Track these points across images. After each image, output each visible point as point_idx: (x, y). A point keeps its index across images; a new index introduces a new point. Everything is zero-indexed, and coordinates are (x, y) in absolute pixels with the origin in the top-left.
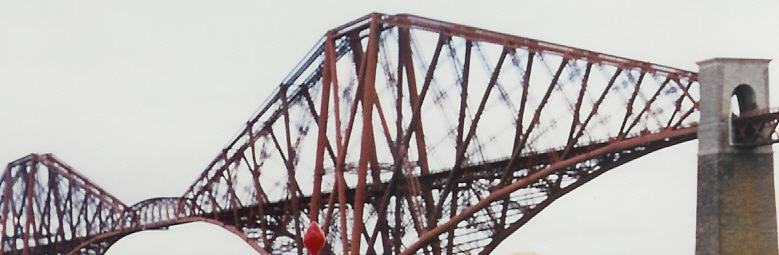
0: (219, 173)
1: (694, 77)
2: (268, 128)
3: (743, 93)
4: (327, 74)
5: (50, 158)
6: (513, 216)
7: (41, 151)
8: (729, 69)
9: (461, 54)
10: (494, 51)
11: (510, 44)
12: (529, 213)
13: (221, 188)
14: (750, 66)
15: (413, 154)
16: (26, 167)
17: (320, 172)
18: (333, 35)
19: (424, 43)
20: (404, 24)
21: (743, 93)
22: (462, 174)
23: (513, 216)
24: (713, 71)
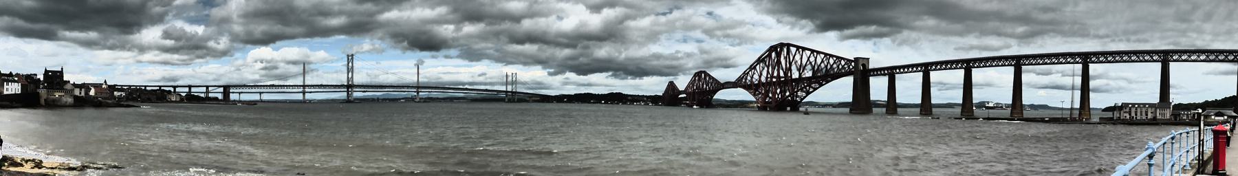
0: (743, 77)
1: (852, 61)
2: (755, 68)
3: (864, 65)
4: (770, 56)
5: (705, 72)
6: (811, 90)
7: (703, 70)
8: (861, 60)
9: (801, 53)
10: (808, 53)
11: (813, 51)
12: (815, 89)
13: (744, 80)
15: (789, 75)
16: (698, 74)
17: (767, 78)
18: (771, 47)
19: (793, 50)
20: (789, 45)
21: (864, 65)
22: (801, 79)
23: (811, 90)
24: (857, 60)
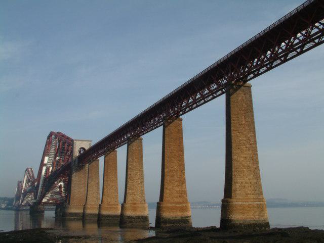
14: (85, 142)
